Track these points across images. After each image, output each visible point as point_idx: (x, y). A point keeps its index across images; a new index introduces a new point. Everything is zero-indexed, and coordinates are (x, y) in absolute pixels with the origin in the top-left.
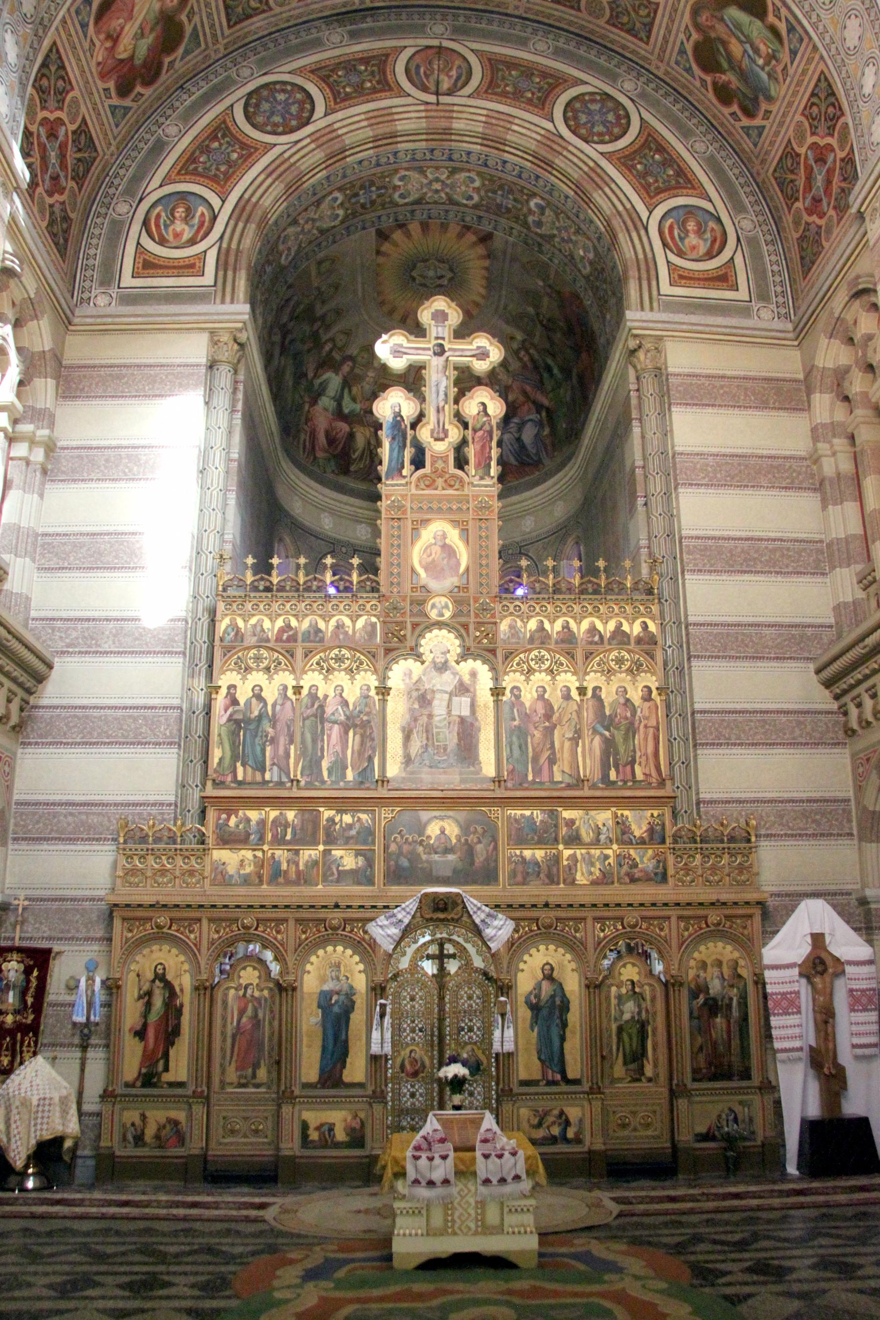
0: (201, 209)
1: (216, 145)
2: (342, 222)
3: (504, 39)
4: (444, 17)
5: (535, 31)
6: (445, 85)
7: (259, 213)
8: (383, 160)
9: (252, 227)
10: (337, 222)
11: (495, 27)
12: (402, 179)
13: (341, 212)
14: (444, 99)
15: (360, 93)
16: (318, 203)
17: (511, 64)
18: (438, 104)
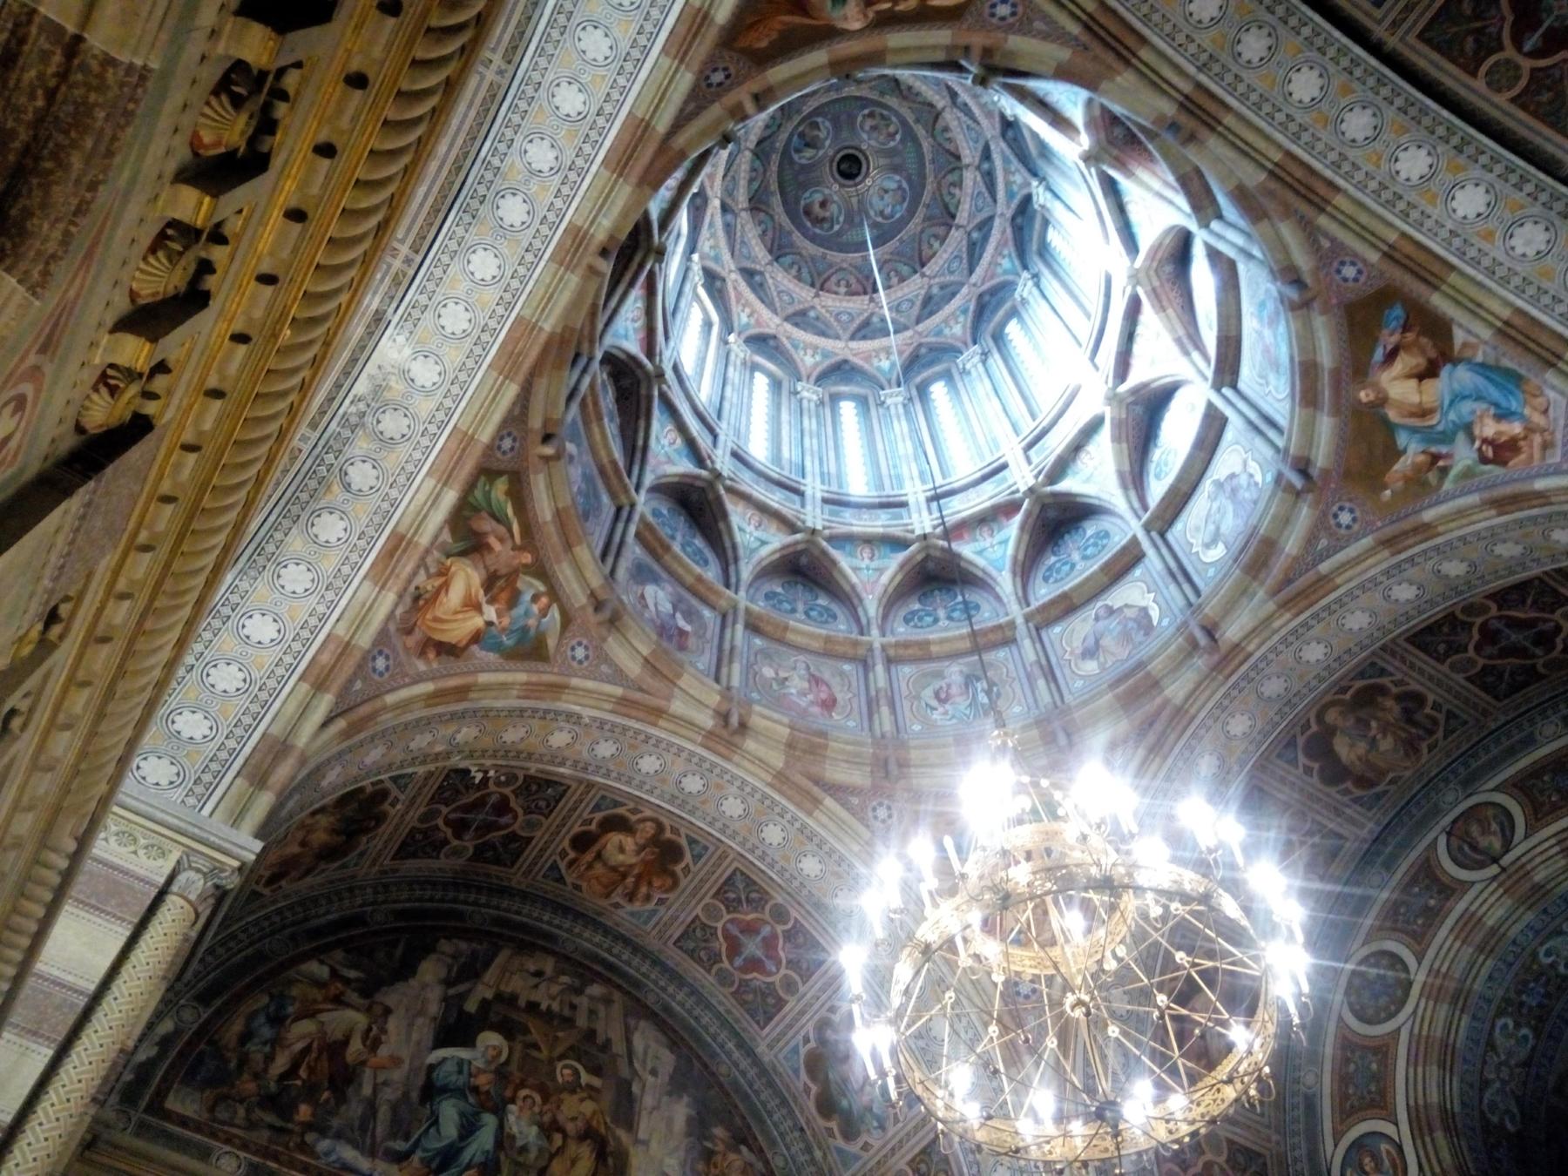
0: (1384, 1147)
1: (1352, 1067)
2: (1537, 1036)
3: (1512, 753)
4: (1446, 781)
5: (1532, 722)
6: (1497, 844)
7: (1435, 1113)
8: (1510, 958)
9: (1439, 1135)
10: (1531, 1042)
11: (1495, 751)
12: (1548, 954)
13: (1525, 1031)
14: (1507, 860)
15: (1433, 917)
16: (1491, 1045)
17: (1536, 772)
18: (1504, 870)
